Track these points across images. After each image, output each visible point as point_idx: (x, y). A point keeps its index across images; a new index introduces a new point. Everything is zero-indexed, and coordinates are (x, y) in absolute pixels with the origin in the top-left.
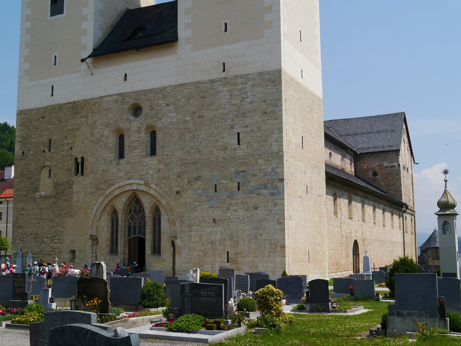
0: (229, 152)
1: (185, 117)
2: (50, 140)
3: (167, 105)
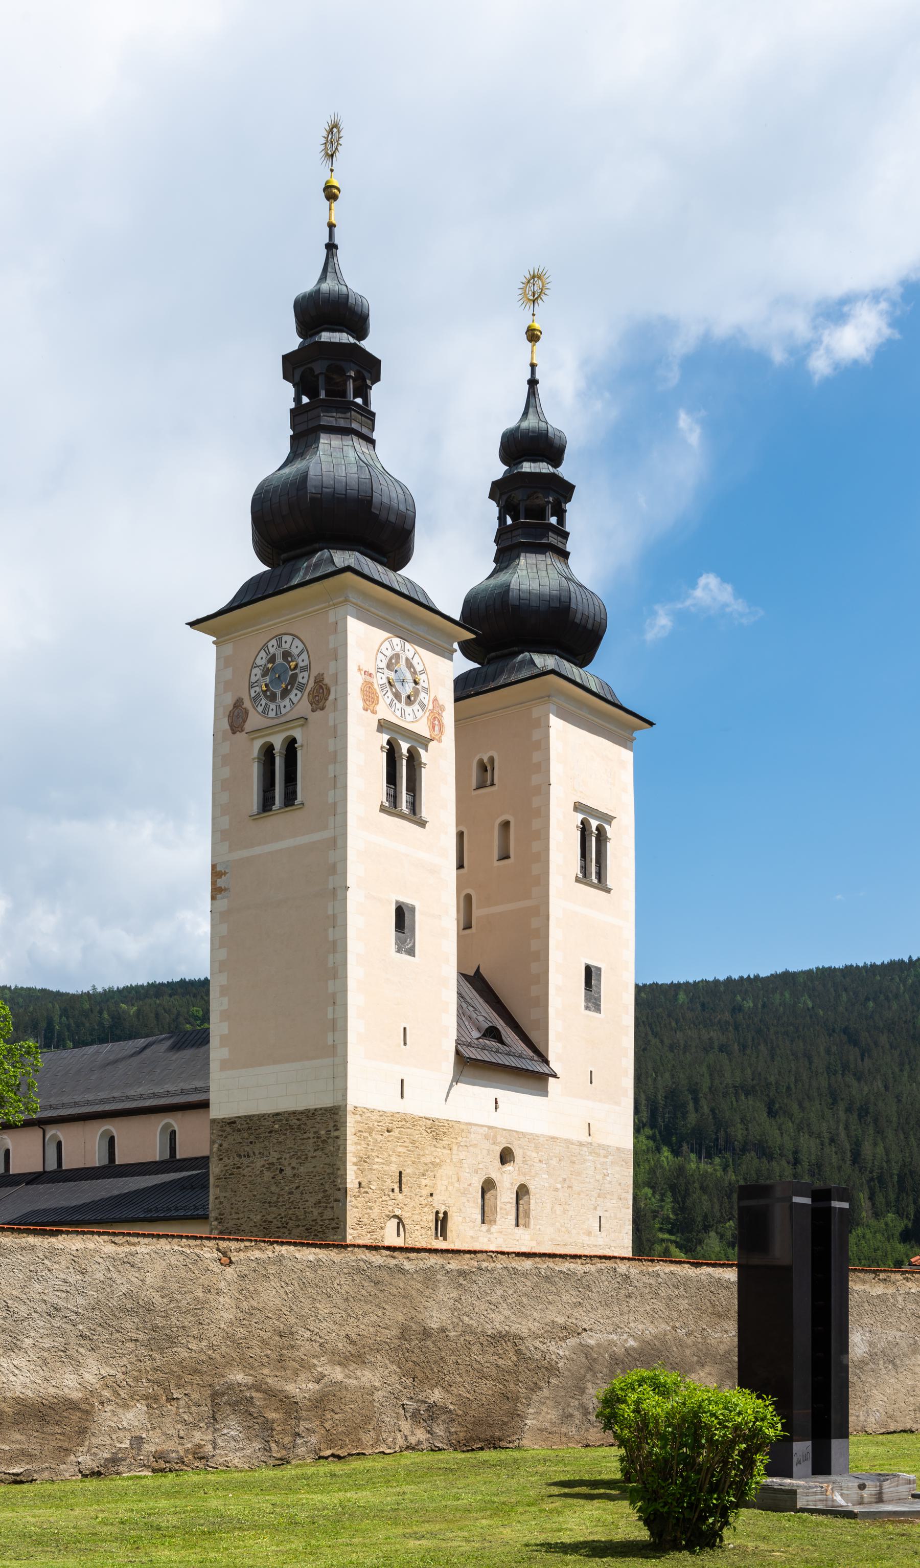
0: (592, 1238)
1: (556, 1183)
2: (401, 1173)
3: (540, 1161)
